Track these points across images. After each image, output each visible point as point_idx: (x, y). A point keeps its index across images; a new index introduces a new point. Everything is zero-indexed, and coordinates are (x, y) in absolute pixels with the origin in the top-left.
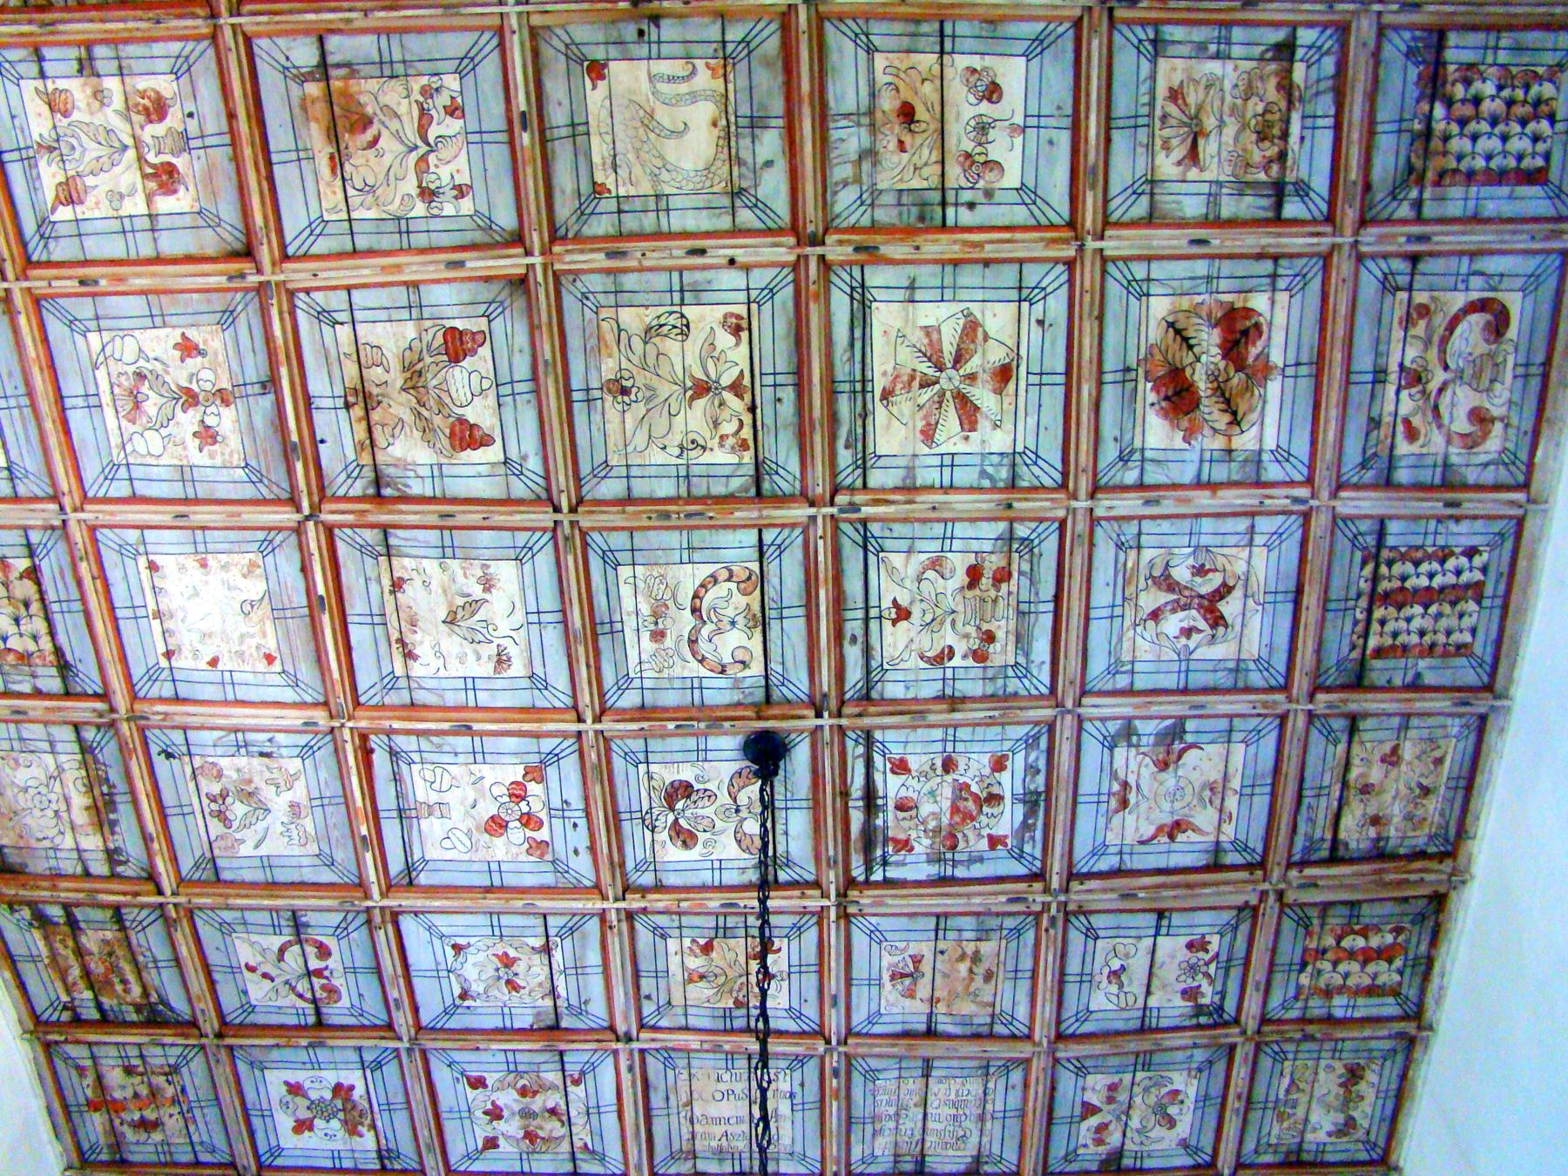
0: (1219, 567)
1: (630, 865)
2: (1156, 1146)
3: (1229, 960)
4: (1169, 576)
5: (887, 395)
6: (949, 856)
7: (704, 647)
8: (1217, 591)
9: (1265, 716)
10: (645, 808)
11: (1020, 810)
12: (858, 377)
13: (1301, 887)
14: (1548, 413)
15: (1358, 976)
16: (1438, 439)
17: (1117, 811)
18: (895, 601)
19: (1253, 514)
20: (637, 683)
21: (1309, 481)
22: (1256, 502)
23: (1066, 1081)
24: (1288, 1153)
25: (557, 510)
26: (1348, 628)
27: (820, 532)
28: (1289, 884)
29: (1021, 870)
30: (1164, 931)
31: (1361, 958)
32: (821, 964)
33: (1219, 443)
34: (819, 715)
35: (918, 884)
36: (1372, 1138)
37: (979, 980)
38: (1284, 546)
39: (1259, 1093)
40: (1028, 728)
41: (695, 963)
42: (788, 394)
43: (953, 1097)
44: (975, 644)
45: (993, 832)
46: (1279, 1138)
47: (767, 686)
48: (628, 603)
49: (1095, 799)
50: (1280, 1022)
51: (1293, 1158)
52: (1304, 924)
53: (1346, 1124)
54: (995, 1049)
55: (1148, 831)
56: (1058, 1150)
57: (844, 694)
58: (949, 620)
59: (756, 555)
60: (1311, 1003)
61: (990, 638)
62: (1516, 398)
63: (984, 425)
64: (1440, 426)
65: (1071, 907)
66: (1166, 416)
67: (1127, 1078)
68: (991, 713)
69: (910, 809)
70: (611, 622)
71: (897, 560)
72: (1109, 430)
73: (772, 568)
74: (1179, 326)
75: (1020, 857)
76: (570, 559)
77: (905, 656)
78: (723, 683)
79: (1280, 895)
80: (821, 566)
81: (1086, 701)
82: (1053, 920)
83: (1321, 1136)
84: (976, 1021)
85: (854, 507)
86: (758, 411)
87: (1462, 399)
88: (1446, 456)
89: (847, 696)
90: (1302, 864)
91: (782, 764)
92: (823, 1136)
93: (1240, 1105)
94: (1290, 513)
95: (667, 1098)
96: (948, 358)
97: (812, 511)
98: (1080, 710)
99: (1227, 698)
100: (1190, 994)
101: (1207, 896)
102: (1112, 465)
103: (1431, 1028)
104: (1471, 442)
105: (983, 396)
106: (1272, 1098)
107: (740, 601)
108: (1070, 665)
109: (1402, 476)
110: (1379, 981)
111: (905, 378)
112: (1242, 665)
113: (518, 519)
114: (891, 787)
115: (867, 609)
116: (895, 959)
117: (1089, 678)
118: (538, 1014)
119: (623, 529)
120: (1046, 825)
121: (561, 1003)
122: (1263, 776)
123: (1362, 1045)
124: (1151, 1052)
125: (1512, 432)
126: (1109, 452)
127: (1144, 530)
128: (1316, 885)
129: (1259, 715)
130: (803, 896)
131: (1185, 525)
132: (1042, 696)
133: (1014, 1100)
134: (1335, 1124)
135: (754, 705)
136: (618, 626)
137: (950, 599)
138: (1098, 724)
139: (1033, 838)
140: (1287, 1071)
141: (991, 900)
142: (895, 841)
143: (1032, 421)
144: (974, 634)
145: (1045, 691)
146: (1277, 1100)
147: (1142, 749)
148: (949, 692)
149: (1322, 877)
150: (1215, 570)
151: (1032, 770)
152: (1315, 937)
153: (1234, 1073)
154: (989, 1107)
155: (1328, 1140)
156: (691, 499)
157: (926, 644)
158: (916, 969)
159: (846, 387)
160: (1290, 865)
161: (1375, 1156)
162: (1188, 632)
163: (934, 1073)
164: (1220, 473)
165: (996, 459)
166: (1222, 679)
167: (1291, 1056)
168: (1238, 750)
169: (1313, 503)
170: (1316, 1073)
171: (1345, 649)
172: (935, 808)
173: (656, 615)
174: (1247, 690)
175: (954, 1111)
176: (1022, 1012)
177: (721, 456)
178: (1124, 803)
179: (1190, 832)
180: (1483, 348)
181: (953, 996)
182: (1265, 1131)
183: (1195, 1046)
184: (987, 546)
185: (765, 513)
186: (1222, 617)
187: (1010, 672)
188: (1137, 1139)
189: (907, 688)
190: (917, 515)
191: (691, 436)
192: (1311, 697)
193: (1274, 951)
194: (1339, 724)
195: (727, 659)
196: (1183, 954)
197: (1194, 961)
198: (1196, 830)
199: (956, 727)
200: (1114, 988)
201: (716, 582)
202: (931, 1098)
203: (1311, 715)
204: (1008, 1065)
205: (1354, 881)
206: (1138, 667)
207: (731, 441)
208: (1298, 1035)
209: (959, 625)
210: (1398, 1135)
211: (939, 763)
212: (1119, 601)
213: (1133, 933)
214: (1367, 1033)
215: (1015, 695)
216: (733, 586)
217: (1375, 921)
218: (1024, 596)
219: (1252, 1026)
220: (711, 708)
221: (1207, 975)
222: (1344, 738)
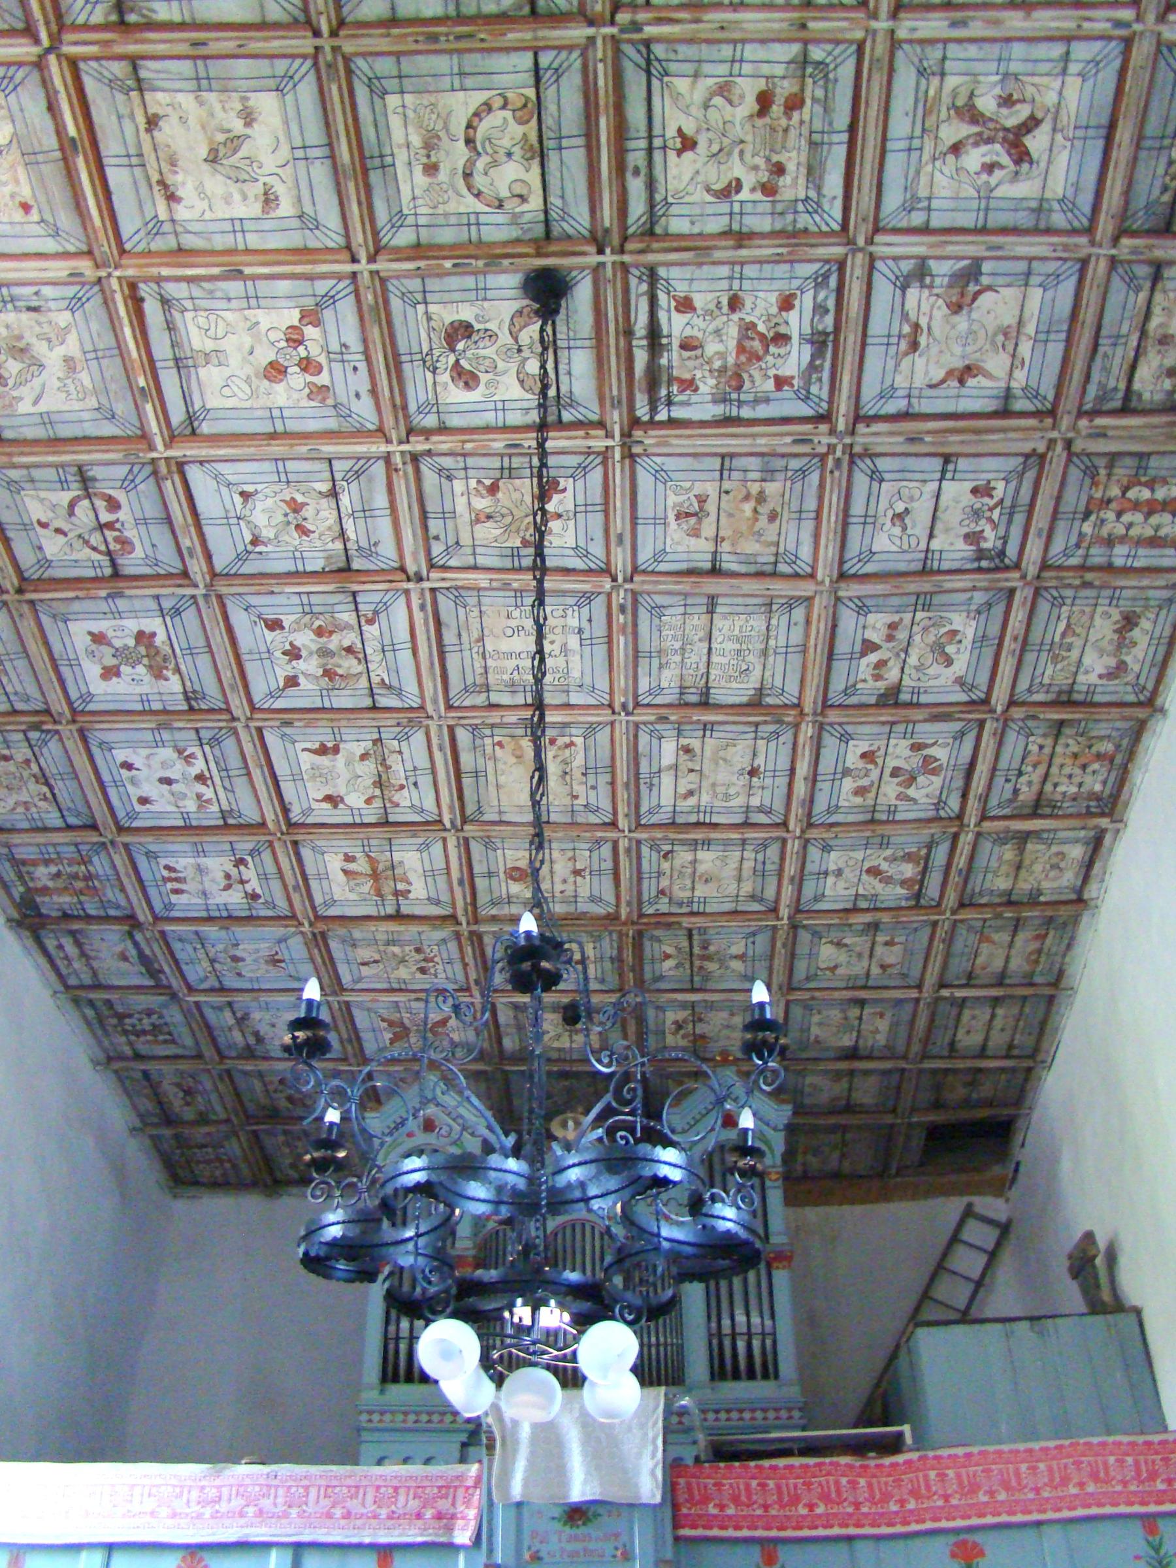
0: (1028, 96)
1: (412, 407)
2: (931, 683)
3: (1013, 506)
4: (973, 107)
6: (734, 396)
7: (479, 181)
8: (1024, 124)
9: (1065, 260)
11: (807, 350)
13: (1090, 436)
15: (1142, 527)
17: (906, 354)
18: (680, 130)
19: (1068, 39)
20: (410, 220)
22: (1072, 25)
23: (848, 619)
24: (1060, 693)
25: (317, 34)
26: (1161, 170)
27: (600, 55)
28: (1078, 432)
29: (807, 411)
30: (949, 475)
31: (1145, 510)
34: (601, 252)
35: (703, 424)
36: (1142, 681)
37: (763, 521)
38: (1100, 76)
39: (1035, 636)
40: (817, 266)
41: (482, 503)
43: (736, 632)
44: (764, 177)
45: (780, 373)
46: (1052, 678)
47: (547, 222)
48: (398, 135)
49: (885, 341)
50: (1060, 568)
51: (1064, 698)
52: (1091, 473)
53: (1118, 668)
54: (780, 588)
55: (938, 374)
56: (838, 684)
57: (626, 229)
58: (736, 151)
59: (532, 81)
60: (1093, 551)
61: (780, 170)
65: (857, 449)
68: (779, 250)
69: (694, 348)
70: (382, 156)
71: (682, 84)
73: (549, 94)
75: (807, 398)
76: (334, 88)
77: (690, 189)
78: (500, 218)
79: (1068, 444)
80: (602, 93)
81: (879, 238)
82: (838, 462)
83: (1093, 678)
84: (761, 559)
85: (636, 27)
89: (631, 231)
91: (563, 303)
93: (1017, 646)
94: (1110, 38)
95: (460, 635)
97: (591, 31)
98: (872, 249)
99: (1027, 239)
100: (973, 538)
101: (994, 442)
106: (1048, 640)
107: (517, 130)
108: (864, 200)
110: (1162, 533)
112: (1045, 205)
113: (276, 45)
114: (676, 325)
115: (650, 137)
117: (882, 216)
119: (389, 54)
120: (834, 366)
122: (1059, 322)
123: (1143, 594)
124: (932, 594)
127: (949, 55)
128: (1105, 435)
129: (1060, 259)
130: (587, 436)
131: (994, 50)
132: (832, 233)
133: (797, 636)
134: (1107, 667)
135: (534, 241)
136: (389, 160)
137: (738, 127)
138: (890, 263)
139: (820, 380)
140: (1064, 616)
141: (776, 441)
142: (681, 381)
144: (763, 166)
145: (836, 227)
147: (936, 291)
148: (736, 227)
150: (1024, 101)
151: (819, 309)
152: (1101, 487)
153: (1013, 614)
154: (772, 642)
156: (461, 19)
157: (712, 177)
158: (701, 509)
160: (1080, 414)
161: (1142, 698)
162: (990, 168)
163: (719, 609)
166: (1024, 219)
167: (1068, 601)
168: (1036, 294)
169: (1137, 27)
170: (1092, 618)
171: (1156, 192)
172: (720, 347)
174: (1048, 231)
175: (737, 646)
176: (805, 552)
178: (914, 346)
179: (980, 378)
181: (738, 535)
182: (1039, 671)
183: (974, 588)
184: (779, 70)
185: (540, 34)
186: (1028, 153)
187: (800, 207)
188: (915, 675)
189: (693, 223)
190: (703, 36)
192: (1115, 240)
193: (1059, 499)
194: (1143, 271)
195: (504, 193)
196: (968, 499)
198: (988, 375)
199: (742, 264)
200: (897, 531)
202: (715, 633)
203: (1113, 262)
204: (791, 604)
205: (1147, 433)
206: (935, 204)
208: (1077, 582)
209: (748, 157)
210: (1166, 680)
211: (725, 301)
212: (918, 132)
213: (918, 476)
214: (1145, 582)
215: (806, 231)
216: (508, 114)
217: (1163, 473)
218: (817, 125)
219: (1032, 571)
221: (990, 520)
222: (1147, 285)
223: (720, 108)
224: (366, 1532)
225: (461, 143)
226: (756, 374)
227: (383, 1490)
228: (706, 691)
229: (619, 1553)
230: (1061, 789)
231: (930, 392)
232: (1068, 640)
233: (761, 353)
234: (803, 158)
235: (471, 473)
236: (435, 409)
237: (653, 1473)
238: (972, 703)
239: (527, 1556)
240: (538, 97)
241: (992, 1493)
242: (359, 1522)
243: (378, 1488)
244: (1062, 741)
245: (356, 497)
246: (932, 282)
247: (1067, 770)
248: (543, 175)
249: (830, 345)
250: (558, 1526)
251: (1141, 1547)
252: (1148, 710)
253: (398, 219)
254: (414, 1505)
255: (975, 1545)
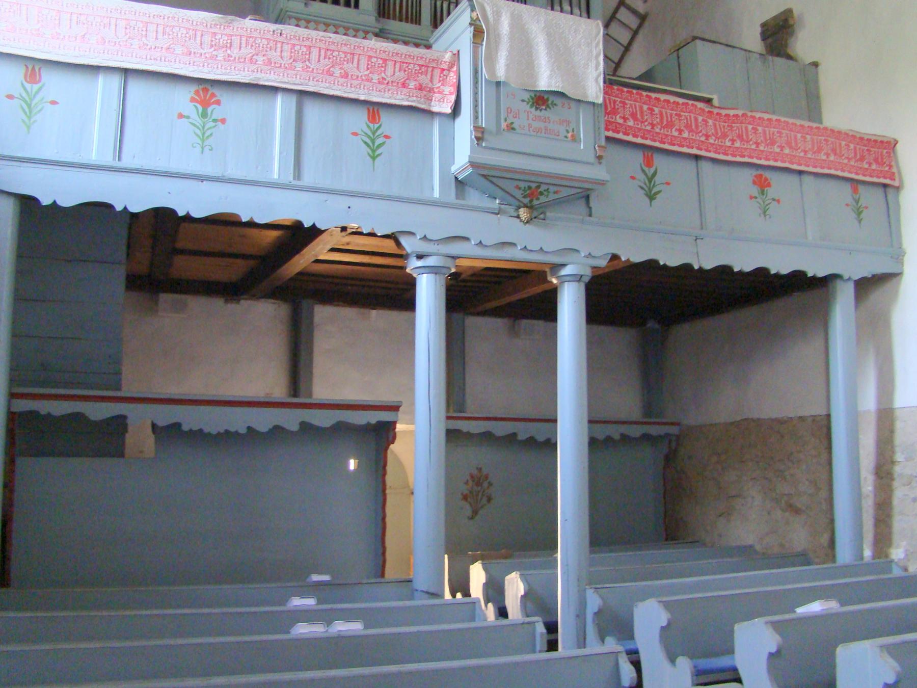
224: (361, 91)
227: (374, 60)
229: (569, 135)
237: (597, 80)
239: (504, 125)
241: (782, 148)
242: (355, 82)
243: (370, 57)
250: (528, 107)
251: (849, 200)
254: (400, 76)
255: (766, 179)
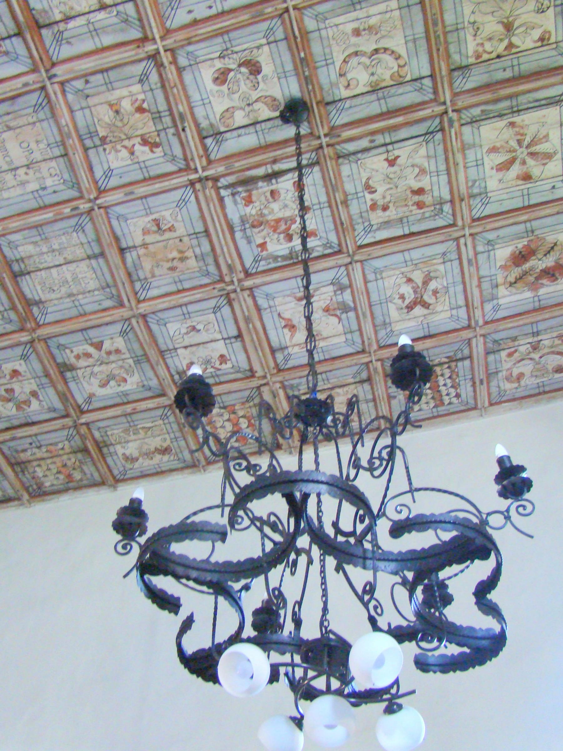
1: (190, 48)
5: (512, 124)
6: (247, 226)
7: (354, 61)
8: (426, 303)
10: (236, 49)
12: (520, 108)
14: (524, 401)
16: (508, 365)
17: (295, 297)
18: (398, 157)
20: (322, 26)
21: (486, 323)
30: (227, 341)
32: (151, 178)
33: (500, 280)
38: (453, 323)
41: (126, 106)
42: (508, 74)
44: (380, 203)
47: (334, 102)
48: (373, 10)
61: (385, 208)
62: (529, 387)
63: (500, 175)
64: (515, 364)
66: (512, 255)
67: (128, 355)
72: (501, 232)
73: (408, 88)
74: (555, 248)
77: (367, 170)
78: (333, 77)
86: (498, 60)
87: (526, 368)
88: (500, 371)
90: (284, 387)
92: (19, 215)
95: (8, 114)
96: (533, 149)
102: (484, 238)
103: (205, 471)
104: (508, 379)
105: (516, 170)
107: (387, 75)
109: (491, 358)
111: (521, 131)
116: (169, 219)
117: (369, 261)
118: (46, 12)
121: (62, 26)
125: (514, 391)
126: (491, 236)
130: (200, 157)
134: (131, 454)
135: (323, 99)
136: (358, 7)
137: (404, 183)
139: (269, 263)
142: (250, 196)
143: (505, 197)
146: (135, 425)
149: (279, 399)
150: (436, 299)
154: (80, 297)
155: (120, 455)
157: (375, 179)
158: (165, 231)
159: (514, 103)
160: (281, 382)
162: (402, 297)
163: (93, 262)
164: (486, 286)
165: (483, 185)
166: (379, 320)
168: (343, 338)
170: (159, 435)
172: (275, 211)
173: (370, 28)
174: (376, 332)
175: (70, 279)
177: (471, 46)
179: (290, 334)
180: (550, 368)
184: (436, 194)
187: (366, 224)
191: (481, 27)
195: (349, 76)
197: (213, 360)
198: (292, 336)
200: (184, 331)
201: (397, 59)
202: (74, 265)
207: (480, 49)
212: (414, 262)
215: (354, 230)
218: (411, 219)
220: (316, 75)
222: (357, 380)
223: (411, 173)
225: (375, 47)
226: (265, 232)
228: (23, 274)
230: (38, 469)
231: (276, 317)
232: (141, 431)
233: (278, 231)
234: (392, 218)
235: (149, 94)
236: (192, 63)
238: (79, 407)
240: (408, 82)
244: (71, 456)
245: (106, 23)
246: (339, 295)
247: (52, 466)
248: (363, 94)
249: (291, 262)
252: (113, 482)
253: (321, 18)
